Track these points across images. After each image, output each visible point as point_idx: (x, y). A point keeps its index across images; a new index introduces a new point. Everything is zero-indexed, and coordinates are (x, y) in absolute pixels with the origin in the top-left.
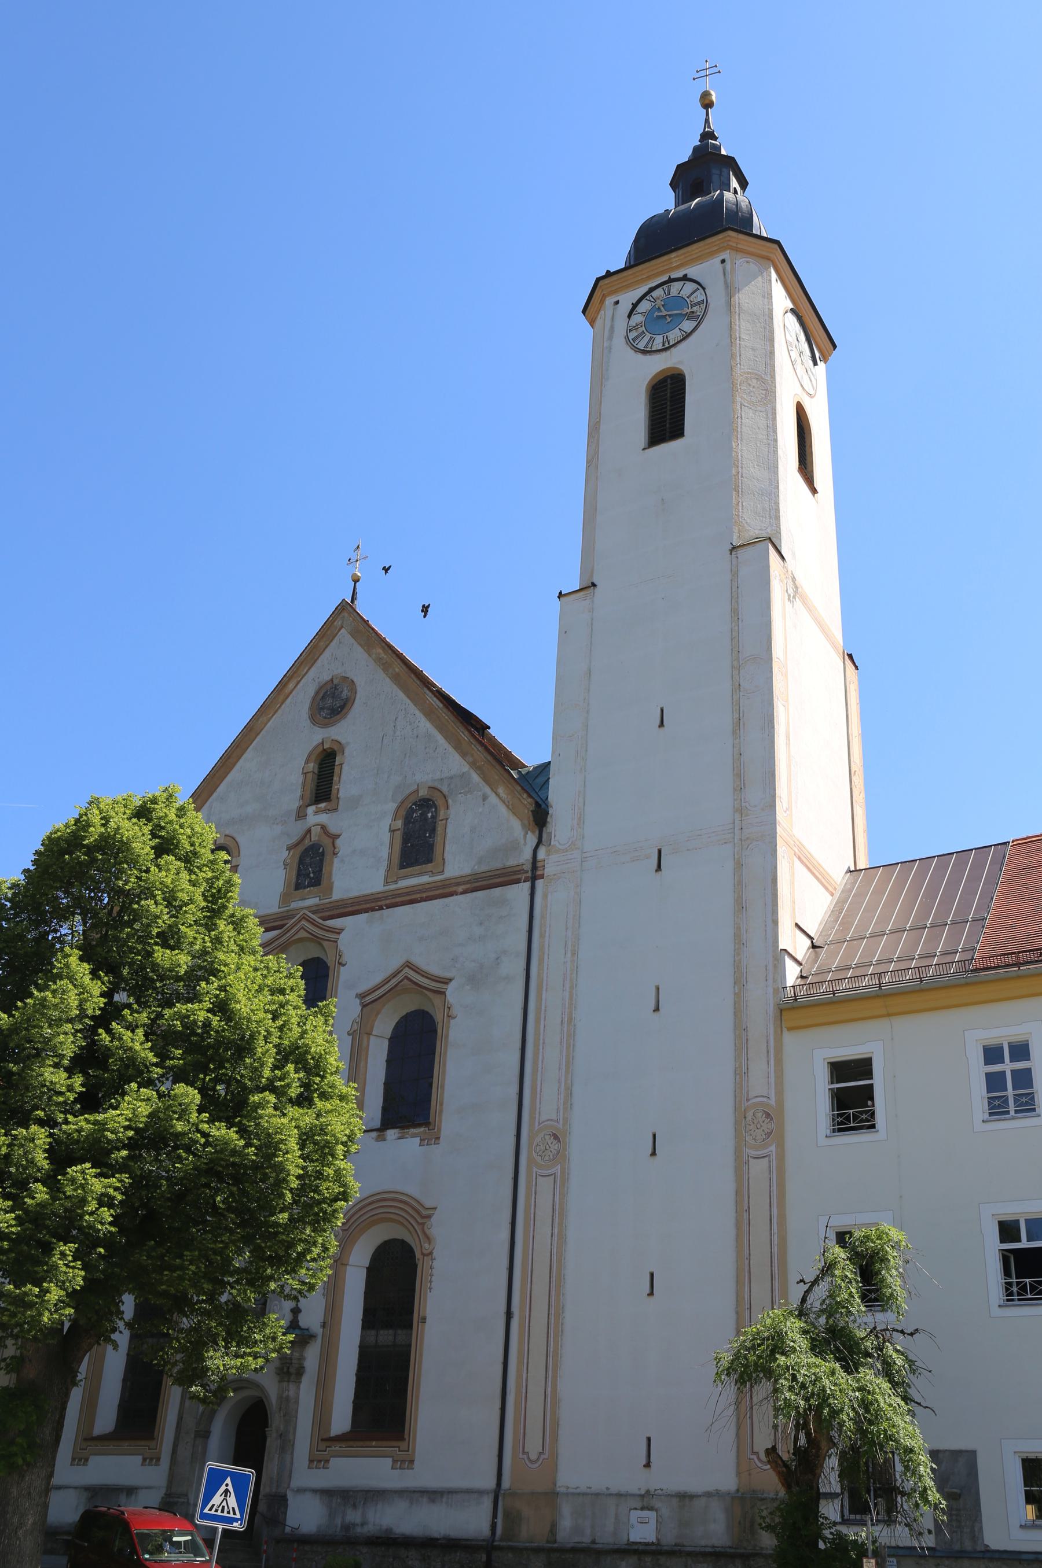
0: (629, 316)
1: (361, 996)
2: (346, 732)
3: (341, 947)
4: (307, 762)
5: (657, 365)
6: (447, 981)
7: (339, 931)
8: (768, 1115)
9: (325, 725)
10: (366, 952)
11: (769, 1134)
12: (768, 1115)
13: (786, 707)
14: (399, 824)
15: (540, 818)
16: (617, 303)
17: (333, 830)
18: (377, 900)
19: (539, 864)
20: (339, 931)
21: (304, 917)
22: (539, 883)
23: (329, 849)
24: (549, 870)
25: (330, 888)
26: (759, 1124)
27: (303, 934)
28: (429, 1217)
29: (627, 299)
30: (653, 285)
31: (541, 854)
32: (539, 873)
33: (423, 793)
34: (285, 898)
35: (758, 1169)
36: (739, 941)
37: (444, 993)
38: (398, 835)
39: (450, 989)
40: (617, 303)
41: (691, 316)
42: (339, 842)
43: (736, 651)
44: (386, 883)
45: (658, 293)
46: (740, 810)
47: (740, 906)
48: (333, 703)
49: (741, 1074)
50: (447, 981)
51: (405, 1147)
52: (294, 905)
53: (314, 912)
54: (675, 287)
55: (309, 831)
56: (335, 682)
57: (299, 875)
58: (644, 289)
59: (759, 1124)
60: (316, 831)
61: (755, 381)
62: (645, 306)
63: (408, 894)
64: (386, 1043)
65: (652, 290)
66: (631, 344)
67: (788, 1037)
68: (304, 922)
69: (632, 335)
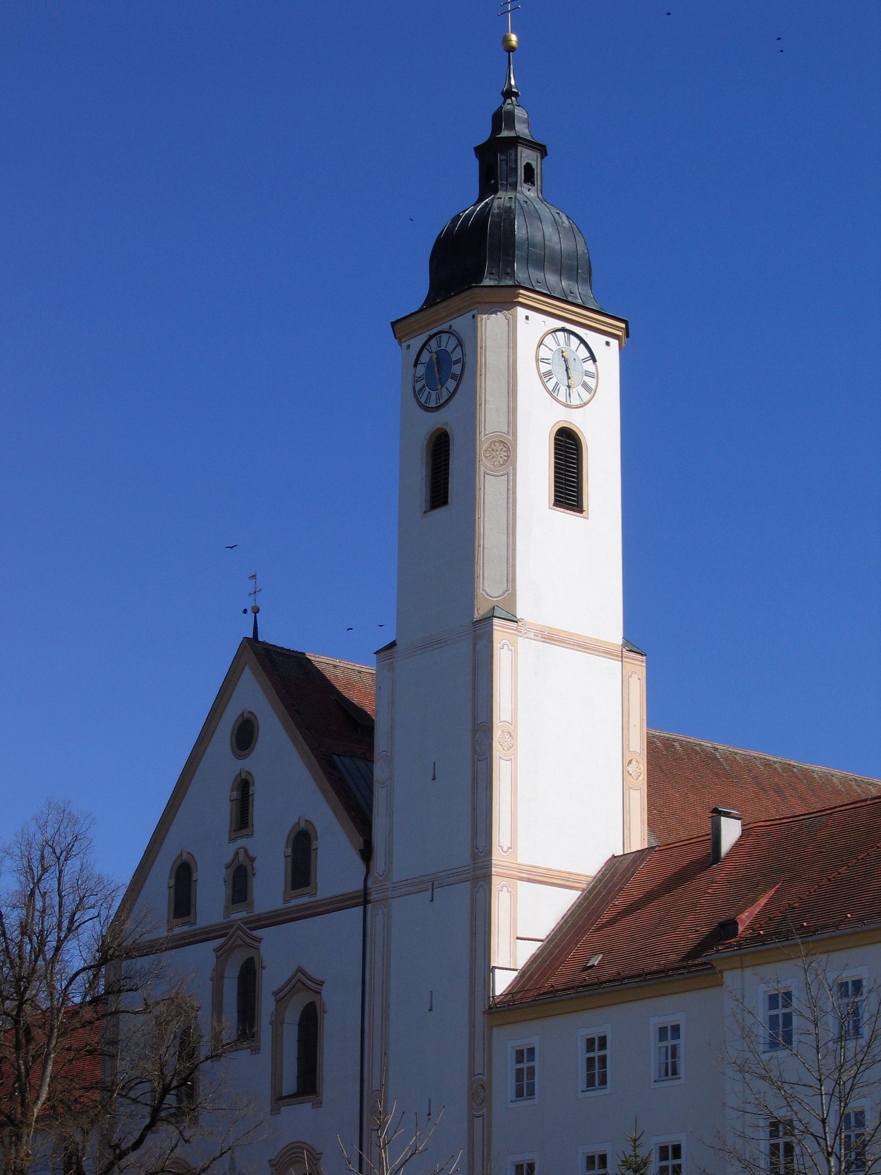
0: (415, 365)
1: (276, 994)
2: (257, 763)
3: (261, 952)
4: (232, 791)
5: (431, 422)
6: (321, 983)
7: (259, 940)
8: (484, 1088)
9: (239, 757)
10: (281, 954)
11: (483, 1101)
12: (484, 1088)
13: (513, 760)
14: (289, 851)
15: (367, 853)
16: (409, 346)
17: (252, 853)
18: (279, 916)
19: (369, 891)
20: (259, 940)
21: (239, 928)
22: (369, 906)
23: (249, 869)
24: (373, 897)
25: (252, 904)
26: (479, 1093)
27: (239, 942)
28: (319, 1159)
29: (417, 342)
30: (432, 332)
31: (370, 885)
32: (369, 898)
33: (303, 825)
34: (227, 912)
35: (478, 1122)
36: (473, 960)
37: (319, 993)
38: (290, 859)
39: (325, 990)
40: (409, 346)
41: (454, 376)
42: (256, 864)
43: (474, 717)
44: (285, 902)
45: (433, 343)
46: (474, 856)
47: (473, 934)
48: (245, 736)
49: (472, 1058)
50: (321, 983)
51: (304, 1109)
52: (233, 917)
53: (245, 923)
54: (445, 336)
55: (237, 853)
56: (246, 716)
57: (234, 891)
58: (424, 337)
59: (479, 1093)
60: (242, 851)
61: (497, 444)
62: (425, 357)
63: (297, 911)
64: (296, 1028)
65: (431, 337)
66: (416, 394)
67: (496, 1031)
68: (239, 932)
69: (418, 386)
